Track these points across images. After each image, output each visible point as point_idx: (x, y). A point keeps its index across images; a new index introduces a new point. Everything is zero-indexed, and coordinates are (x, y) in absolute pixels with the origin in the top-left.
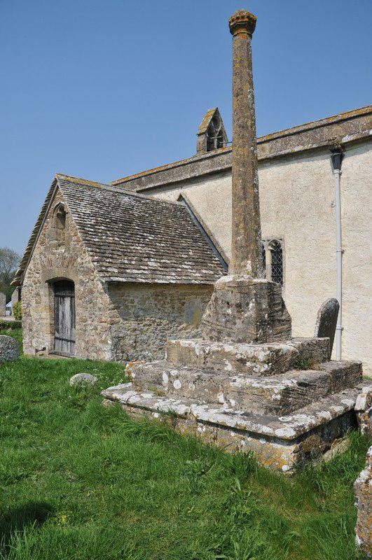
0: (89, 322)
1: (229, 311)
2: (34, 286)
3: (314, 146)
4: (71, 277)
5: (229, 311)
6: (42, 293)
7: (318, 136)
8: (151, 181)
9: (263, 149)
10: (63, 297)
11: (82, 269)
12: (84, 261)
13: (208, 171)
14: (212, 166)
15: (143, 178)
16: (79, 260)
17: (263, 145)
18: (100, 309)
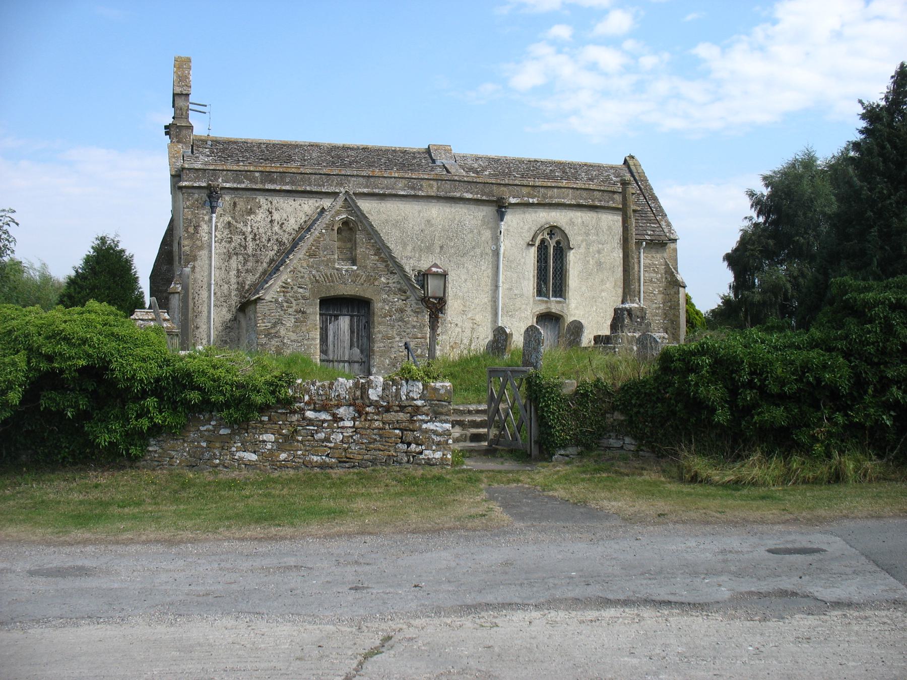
0: (398, 339)
1: (639, 320)
2: (294, 303)
3: (484, 198)
4: (367, 295)
5: (639, 320)
6: (309, 310)
7: (487, 190)
8: (272, 181)
9: (431, 187)
10: (336, 317)
11: (388, 289)
12: (390, 281)
13: (366, 190)
14: (367, 187)
15: (257, 174)
16: (383, 279)
17: (432, 182)
18: (414, 327)
